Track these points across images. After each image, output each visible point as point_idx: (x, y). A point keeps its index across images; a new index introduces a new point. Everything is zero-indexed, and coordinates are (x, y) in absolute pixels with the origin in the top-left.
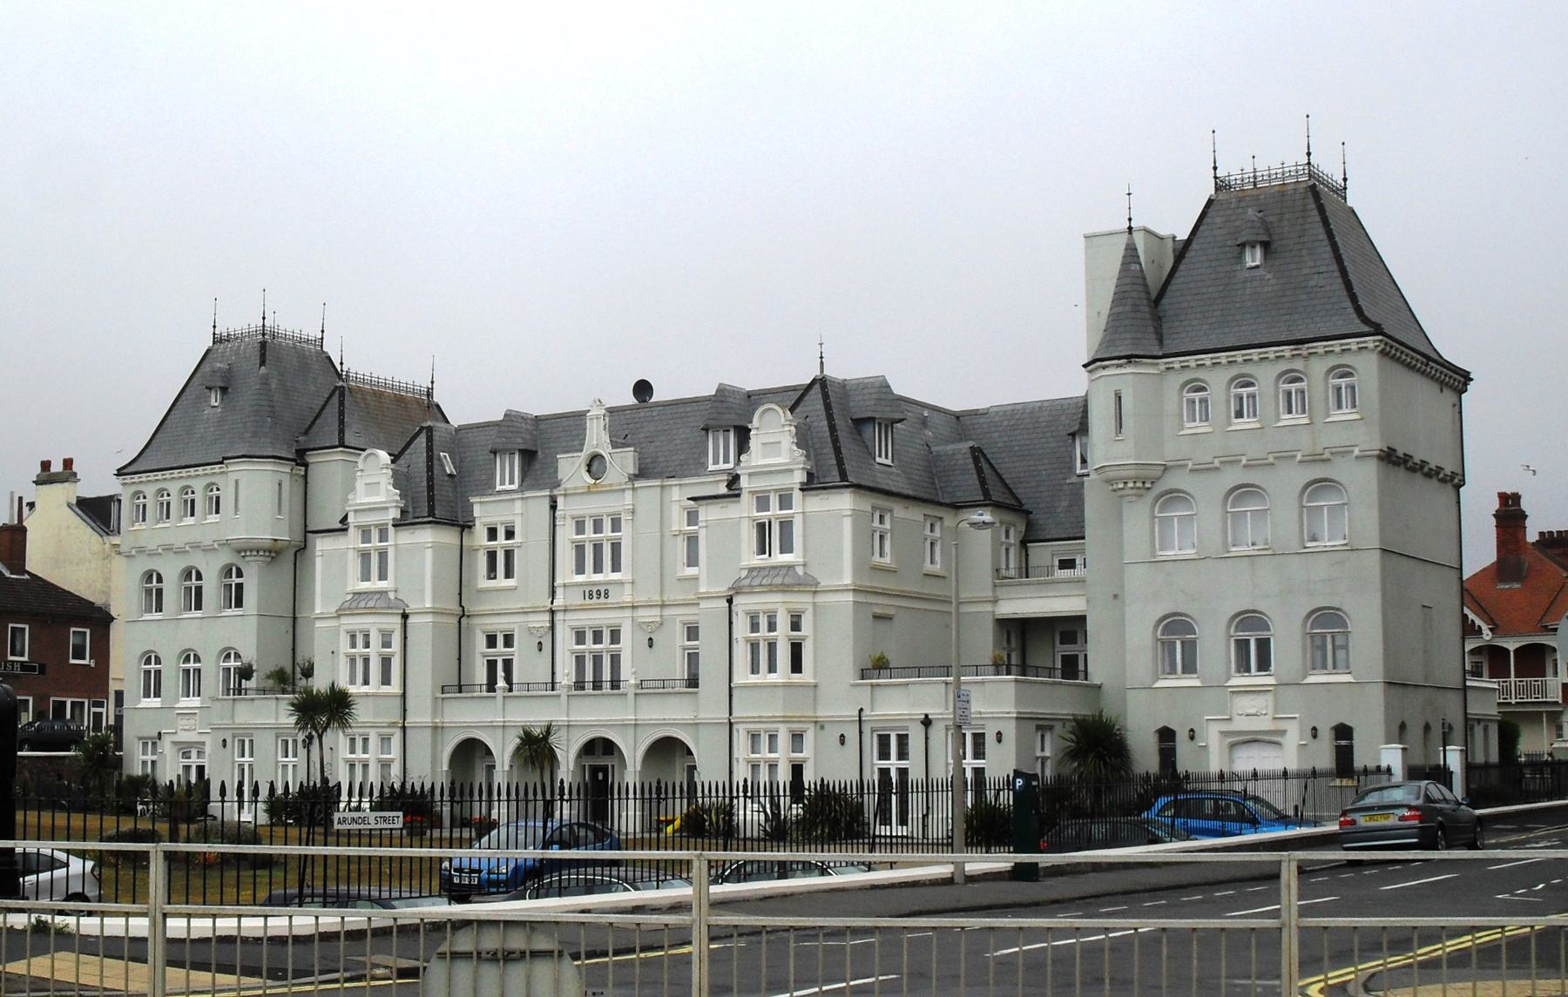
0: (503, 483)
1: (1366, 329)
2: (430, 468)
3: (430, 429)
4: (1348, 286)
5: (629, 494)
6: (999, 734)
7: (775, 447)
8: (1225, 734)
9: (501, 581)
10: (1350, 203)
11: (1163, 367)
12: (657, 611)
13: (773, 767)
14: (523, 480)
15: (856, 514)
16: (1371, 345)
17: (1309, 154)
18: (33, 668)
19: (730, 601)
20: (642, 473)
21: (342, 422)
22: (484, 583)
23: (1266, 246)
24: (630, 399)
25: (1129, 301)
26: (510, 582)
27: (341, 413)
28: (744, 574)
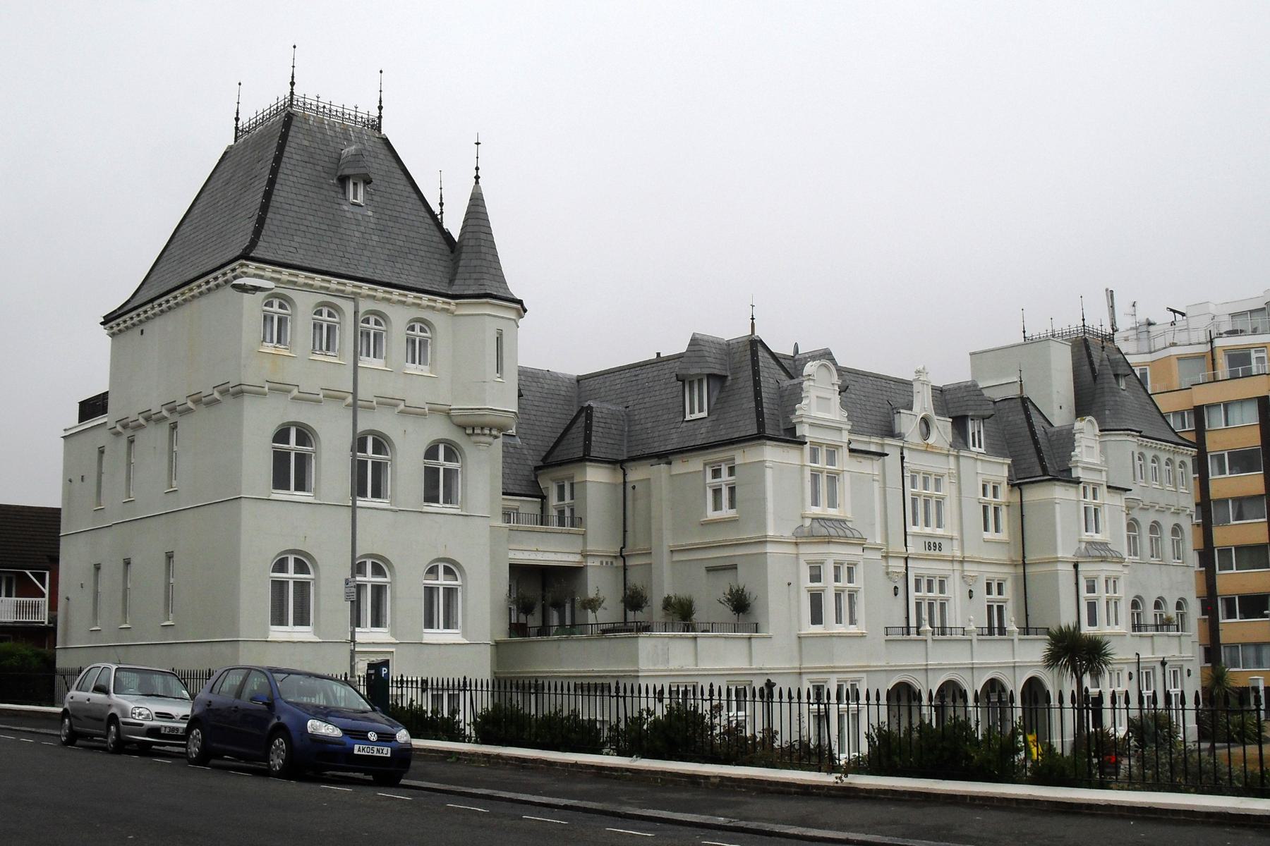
19: (1076, 566)
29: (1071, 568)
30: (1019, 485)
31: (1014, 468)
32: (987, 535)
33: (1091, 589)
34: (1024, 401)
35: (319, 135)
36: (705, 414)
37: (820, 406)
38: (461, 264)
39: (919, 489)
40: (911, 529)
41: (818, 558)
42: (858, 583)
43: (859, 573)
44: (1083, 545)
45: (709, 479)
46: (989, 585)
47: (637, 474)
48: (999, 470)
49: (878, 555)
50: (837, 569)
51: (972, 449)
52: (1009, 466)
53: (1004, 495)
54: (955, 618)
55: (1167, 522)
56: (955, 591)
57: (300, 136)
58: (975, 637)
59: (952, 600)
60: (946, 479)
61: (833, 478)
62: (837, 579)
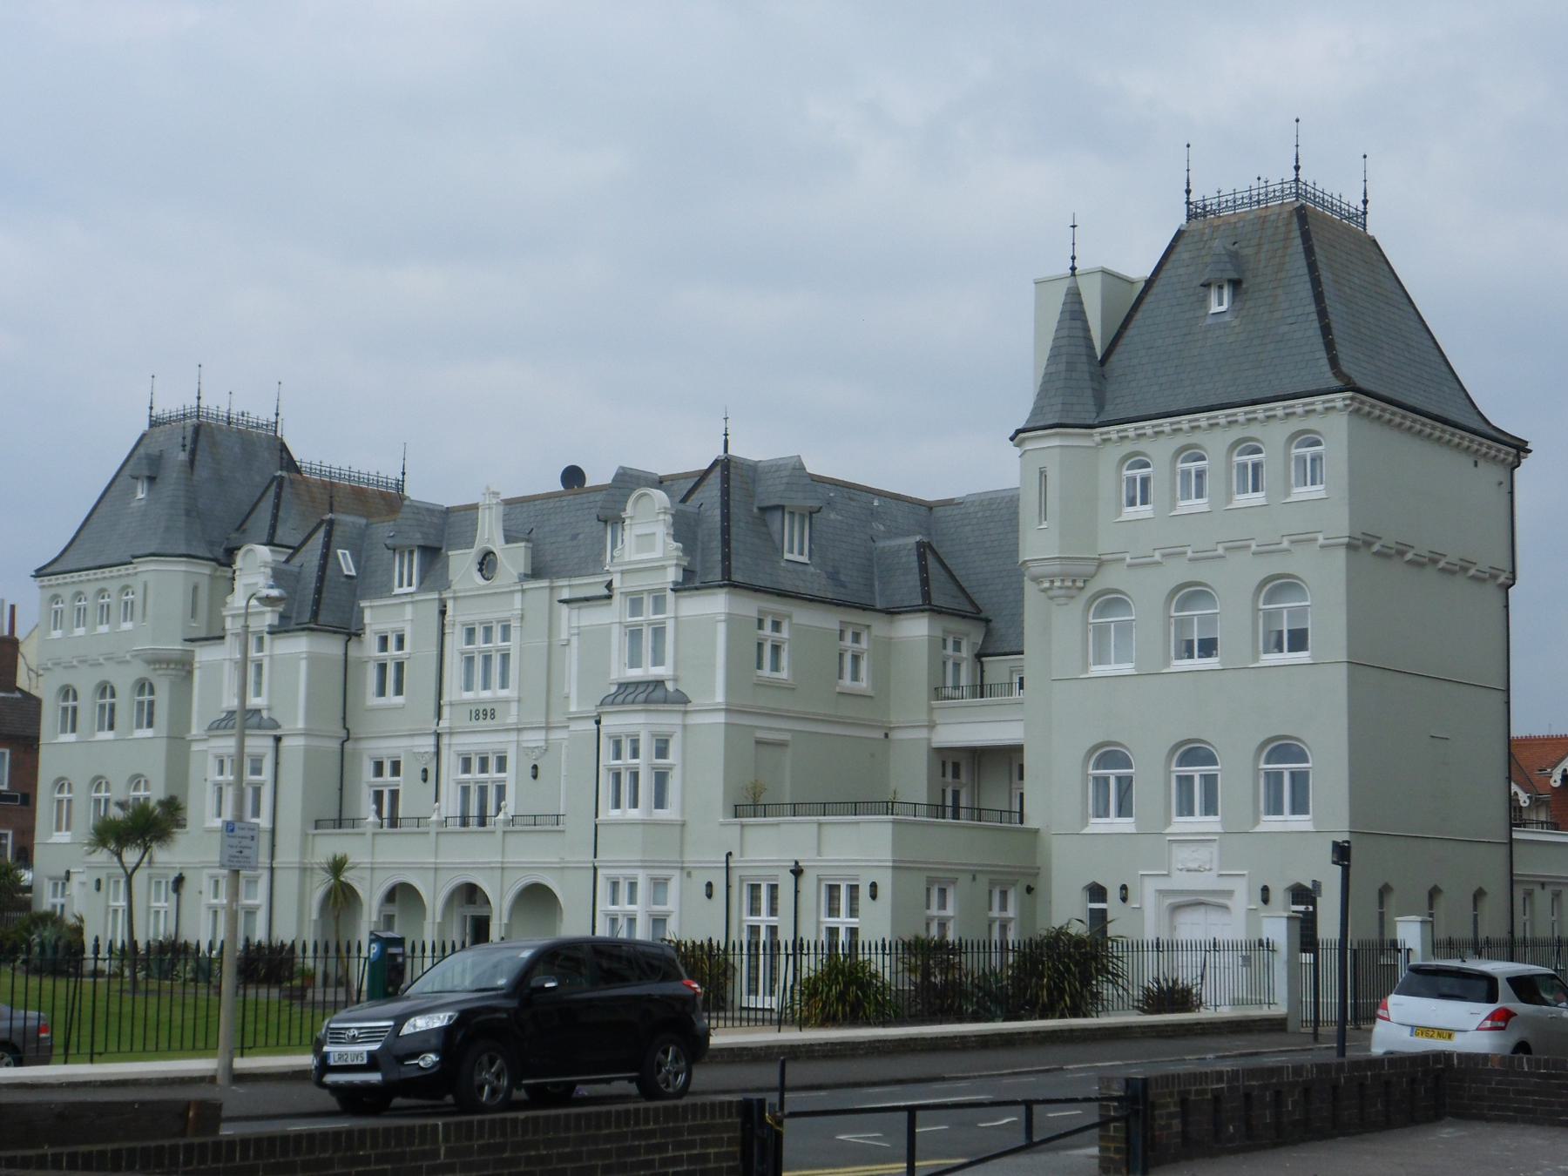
0: (401, 585)
1: (1337, 383)
2: (323, 568)
3: (331, 523)
4: (1326, 330)
5: (518, 596)
6: (874, 886)
7: (647, 542)
8: (1162, 893)
9: (391, 699)
10: (1370, 232)
11: (1098, 438)
12: (541, 735)
13: (632, 921)
14: (421, 582)
15: (731, 619)
16: (1339, 404)
17: (1297, 168)
18: (14, 799)
19: (598, 722)
20: (536, 573)
21: (275, 517)
22: (373, 700)
23: (1236, 284)
24: (558, 486)
25: (1064, 359)
26: (400, 700)
27: (277, 507)
28: (614, 689)
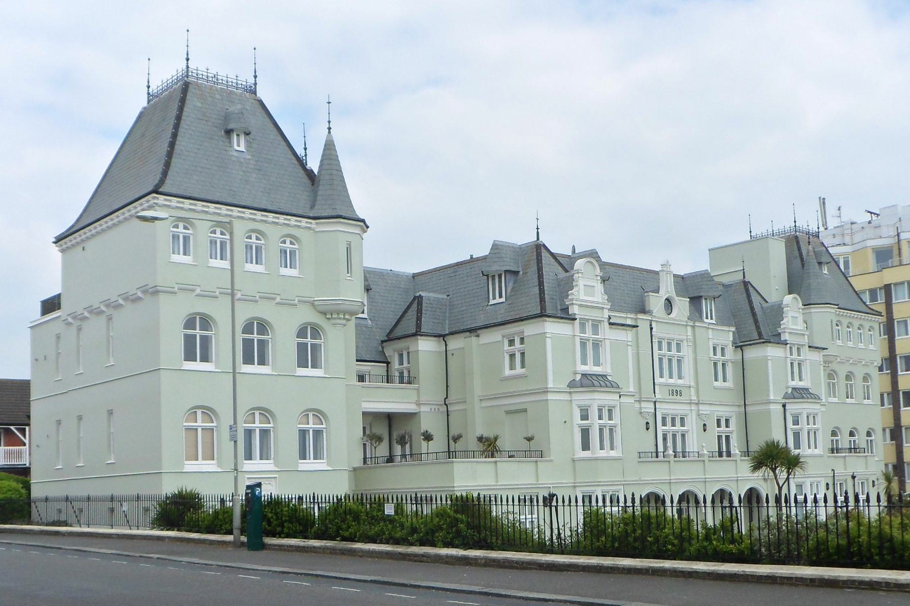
19: (784, 406)
29: (780, 407)
30: (741, 347)
31: (738, 334)
32: (716, 384)
33: (796, 422)
34: (746, 284)
35: (210, 99)
36: (503, 300)
37: (587, 292)
38: (319, 192)
39: (665, 350)
40: (658, 380)
41: (587, 403)
42: (616, 421)
43: (616, 414)
44: (790, 391)
45: (506, 347)
46: (719, 421)
47: (455, 343)
48: (726, 336)
49: (631, 400)
50: (600, 410)
51: (706, 320)
52: (734, 333)
53: (731, 354)
54: (692, 445)
55: (859, 373)
56: (692, 426)
57: (195, 99)
58: (706, 458)
59: (690, 432)
60: (685, 343)
61: (596, 345)
62: (600, 418)
